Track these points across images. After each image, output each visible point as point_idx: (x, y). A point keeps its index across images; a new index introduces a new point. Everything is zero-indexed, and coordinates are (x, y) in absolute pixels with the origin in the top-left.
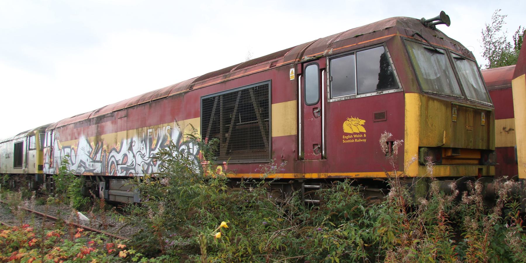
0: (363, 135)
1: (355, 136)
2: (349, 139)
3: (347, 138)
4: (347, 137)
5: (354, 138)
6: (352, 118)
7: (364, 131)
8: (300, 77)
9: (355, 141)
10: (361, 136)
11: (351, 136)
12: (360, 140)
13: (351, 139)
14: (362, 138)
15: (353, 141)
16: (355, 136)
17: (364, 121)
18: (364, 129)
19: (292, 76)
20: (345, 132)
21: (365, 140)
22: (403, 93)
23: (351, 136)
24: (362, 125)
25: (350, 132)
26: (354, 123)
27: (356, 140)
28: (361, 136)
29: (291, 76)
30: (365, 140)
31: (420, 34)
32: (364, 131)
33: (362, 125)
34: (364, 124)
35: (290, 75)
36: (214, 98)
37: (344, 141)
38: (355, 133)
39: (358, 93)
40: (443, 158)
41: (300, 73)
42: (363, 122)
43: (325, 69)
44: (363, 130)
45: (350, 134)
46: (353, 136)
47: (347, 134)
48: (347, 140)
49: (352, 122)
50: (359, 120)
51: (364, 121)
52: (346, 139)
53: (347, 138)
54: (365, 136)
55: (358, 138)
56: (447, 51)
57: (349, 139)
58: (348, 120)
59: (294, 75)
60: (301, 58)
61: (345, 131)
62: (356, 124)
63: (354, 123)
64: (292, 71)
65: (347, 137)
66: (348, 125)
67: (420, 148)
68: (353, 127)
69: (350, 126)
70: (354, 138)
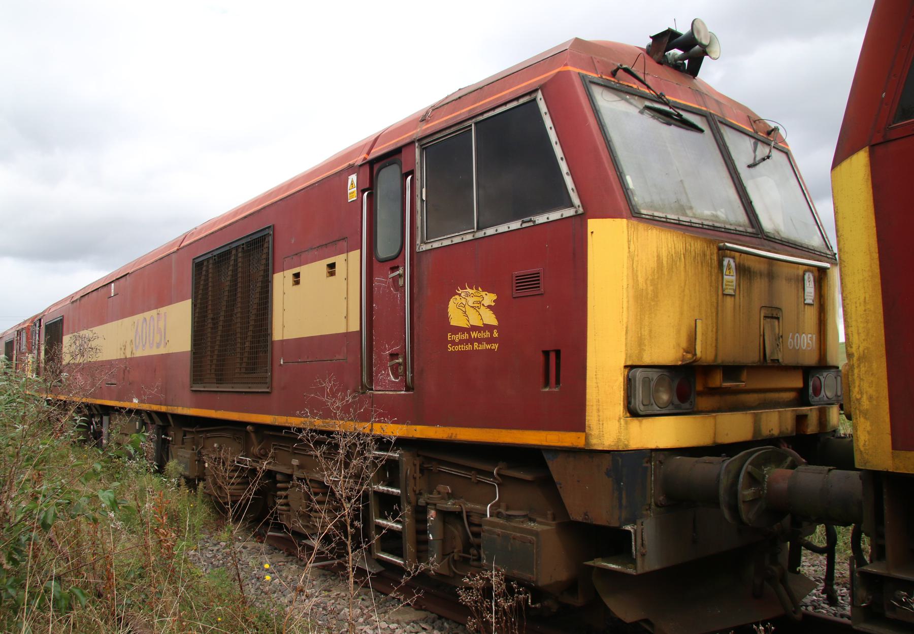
0: (492, 333)
1: (474, 335)
3: (457, 340)
4: (457, 337)
5: (471, 341)
6: (469, 290)
8: (366, 194)
9: (473, 347)
10: (487, 334)
11: (465, 336)
12: (485, 346)
14: (490, 340)
15: (469, 347)
16: (474, 335)
17: (493, 297)
18: (494, 316)
19: (353, 192)
20: (451, 324)
21: (495, 346)
22: (581, 220)
23: (465, 336)
24: (489, 307)
25: (463, 324)
26: (471, 301)
28: (487, 334)
29: (350, 194)
30: (495, 346)
31: (643, 79)
33: (489, 307)
34: (493, 304)
35: (349, 192)
36: (228, 252)
37: (450, 348)
38: (474, 328)
39: (480, 225)
40: (700, 394)
41: (367, 186)
42: (489, 298)
43: (412, 172)
44: (490, 319)
46: (470, 336)
47: (458, 330)
48: (458, 344)
49: (468, 298)
50: (483, 293)
51: (493, 297)
52: (453, 343)
53: (457, 340)
54: (496, 334)
55: (479, 341)
56: (710, 119)
57: (461, 342)
58: (460, 295)
59: (355, 189)
60: (368, 153)
61: (453, 323)
62: (476, 305)
63: (471, 301)
64: (353, 178)
66: (458, 307)
67: (630, 367)
68: (471, 312)
69: (464, 309)
70: (471, 341)
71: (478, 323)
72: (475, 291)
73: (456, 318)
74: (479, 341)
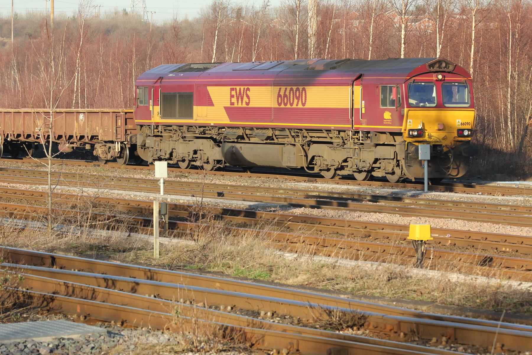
5: (387, 122)
14: (390, 122)
38: (388, 119)
42: (390, 114)
47: (385, 119)
70: (387, 122)
73: (385, 117)
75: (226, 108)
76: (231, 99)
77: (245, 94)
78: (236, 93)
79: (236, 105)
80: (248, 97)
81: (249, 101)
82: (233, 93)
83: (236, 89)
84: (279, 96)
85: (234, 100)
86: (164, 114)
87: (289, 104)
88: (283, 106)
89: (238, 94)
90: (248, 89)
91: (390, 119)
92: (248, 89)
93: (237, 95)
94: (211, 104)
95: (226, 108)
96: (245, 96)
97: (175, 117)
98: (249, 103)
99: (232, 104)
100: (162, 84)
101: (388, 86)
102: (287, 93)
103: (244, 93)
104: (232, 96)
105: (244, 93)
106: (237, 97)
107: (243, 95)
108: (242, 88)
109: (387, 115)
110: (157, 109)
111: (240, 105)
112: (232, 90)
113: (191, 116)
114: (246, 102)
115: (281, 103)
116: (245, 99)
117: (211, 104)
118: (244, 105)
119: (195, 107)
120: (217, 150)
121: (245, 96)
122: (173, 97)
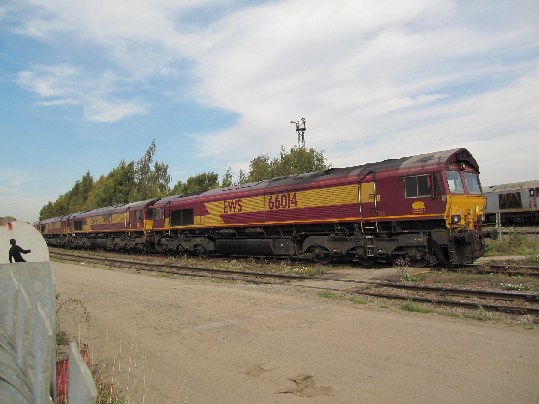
0: (424, 210)
1: (419, 210)
2: (416, 212)
4: (415, 211)
5: (418, 211)
7: (424, 208)
10: (423, 210)
11: (417, 210)
13: (417, 211)
14: (423, 211)
15: (418, 212)
16: (419, 210)
23: (417, 210)
24: (423, 205)
27: (420, 212)
28: (423, 210)
32: (424, 208)
33: (423, 205)
42: (423, 203)
44: (424, 207)
45: (416, 209)
47: (415, 209)
50: (421, 202)
52: (414, 212)
54: (424, 210)
55: (421, 211)
57: (416, 212)
65: (415, 211)
68: (418, 206)
70: (418, 211)
71: (421, 208)
72: (419, 202)
74: (421, 211)
75: (220, 216)
76: (224, 208)
77: (237, 204)
78: (229, 204)
79: (229, 213)
80: (240, 206)
81: (241, 208)
82: (227, 204)
83: (229, 201)
84: (270, 201)
85: (228, 209)
86: (172, 224)
87: (281, 207)
88: (275, 209)
89: (230, 205)
90: (241, 201)
91: (422, 209)
92: (241, 201)
93: (229, 205)
94: (208, 214)
95: (220, 216)
96: (237, 205)
97: (181, 224)
98: (241, 209)
99: (227, 212)
100: (171, 205)
101: (417, 176)
102: (279, 199)
103: (236, 203)
104: (225, 207)
105: (236, 203)
106: (229, 207)
107: (236, 205)
108: (234, 201)
109: (418, 205)
110: (168, 220)
111: (233, 212)
112: (225, 203)
113: (192, 223)
114: (238, 210)
115: (273, 207)
116: (238, 207)
117: (208, 214)
118: (237, 212)
119: (194, 217)
120: (212, 244)
121: (237, 205)
122: (178, 212)
